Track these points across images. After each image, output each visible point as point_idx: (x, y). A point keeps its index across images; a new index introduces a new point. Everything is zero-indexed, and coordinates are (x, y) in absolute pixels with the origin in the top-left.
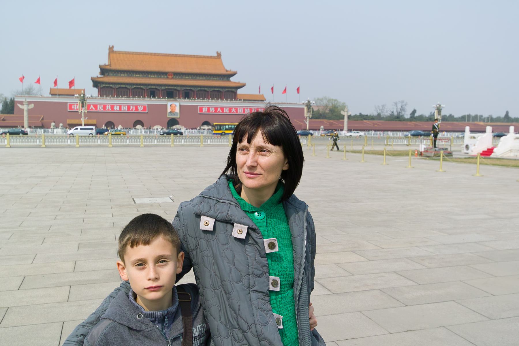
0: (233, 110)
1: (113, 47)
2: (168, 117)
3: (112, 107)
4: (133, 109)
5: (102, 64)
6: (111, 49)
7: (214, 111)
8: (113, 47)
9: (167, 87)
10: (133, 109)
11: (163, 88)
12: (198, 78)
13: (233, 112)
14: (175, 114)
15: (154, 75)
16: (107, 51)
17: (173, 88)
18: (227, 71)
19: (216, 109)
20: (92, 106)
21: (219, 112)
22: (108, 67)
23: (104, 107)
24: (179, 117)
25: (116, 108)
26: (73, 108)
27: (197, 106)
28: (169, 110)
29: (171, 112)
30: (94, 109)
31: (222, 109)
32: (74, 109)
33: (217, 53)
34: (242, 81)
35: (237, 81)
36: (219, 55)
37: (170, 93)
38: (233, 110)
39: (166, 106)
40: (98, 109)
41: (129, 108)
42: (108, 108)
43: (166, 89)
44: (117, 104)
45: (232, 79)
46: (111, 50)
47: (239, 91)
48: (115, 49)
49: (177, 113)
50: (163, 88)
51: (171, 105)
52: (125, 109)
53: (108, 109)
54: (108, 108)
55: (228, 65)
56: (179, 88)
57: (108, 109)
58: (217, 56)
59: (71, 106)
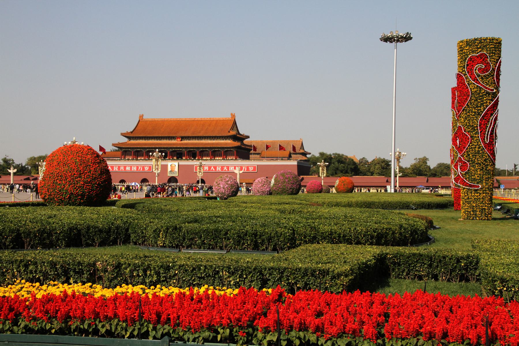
0: (225, 168)
3: (125, 168)
5: (125, 132)
6: (141, 117)
8: (143, 116)
19: (210, 168)
21: (212, 170)
22: (131, 135)
25: (128, 168)
28: (169, 169)
29: (171, 171)
33: (232, 114)
36: (233, 116)
38: (225, 168)
39: (167, 166)
41: (137, 168)
42: (122, 168)
44: (129, 165)
46: (141, 117)
52: (134, 169)
54: (122, 168)
58: (232, 117)
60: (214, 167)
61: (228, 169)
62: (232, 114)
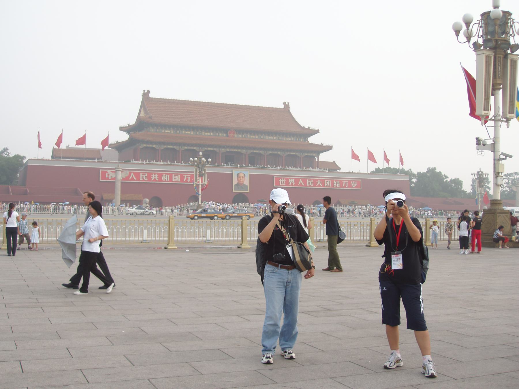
1: (148, 92)
2: (234, 191)
3: (160, 176)
4: (187, 179)
6: (146, 95)
7: (294, 183)
8: (148, 92)
9: (228, 150)
10: (187, 179)
11: (223, 150)
12: (267, 137)
13: (319, 185)
14: (243, 187)
15: (209, 132)
16: (141, 98)
17: (236, 150)
18: (304, 128)
19: (297, 181)
20: (132, 174)
21: (301, 185)
23: (149, 176)
24: (248, 192)
25: (165, 178)
26: (107, 177)
27: (273, 176)
28: (235, 182)
29: (237, 185)
30: (135, 179)
31: (305, 181)
32: (108, 179)
33: (285, 103)
34: (326, 143)
35: (319, 143)
36: (287, 106)
37: (231, 159)
39: (232, 174)
40: (141, 179)
41: (182, 178)
42: (155, 177)
43: (227, 151)
45: (312, 140)
47: (324, 157)
48: (151, 96)
49: (247, 186)
50: (223, 150)
51: (238, 175)
52: (177, 179)
53: (155, 180)
55: (303, 118)
56: (244, 151)
57: (155, 180)
59: (104, 173)
60: (303, 180)
61: (323, 184)
62: (285, 103)
